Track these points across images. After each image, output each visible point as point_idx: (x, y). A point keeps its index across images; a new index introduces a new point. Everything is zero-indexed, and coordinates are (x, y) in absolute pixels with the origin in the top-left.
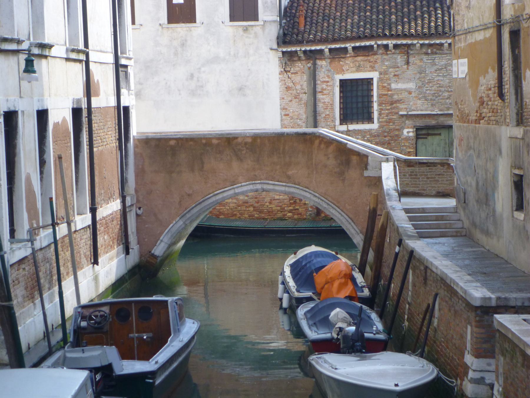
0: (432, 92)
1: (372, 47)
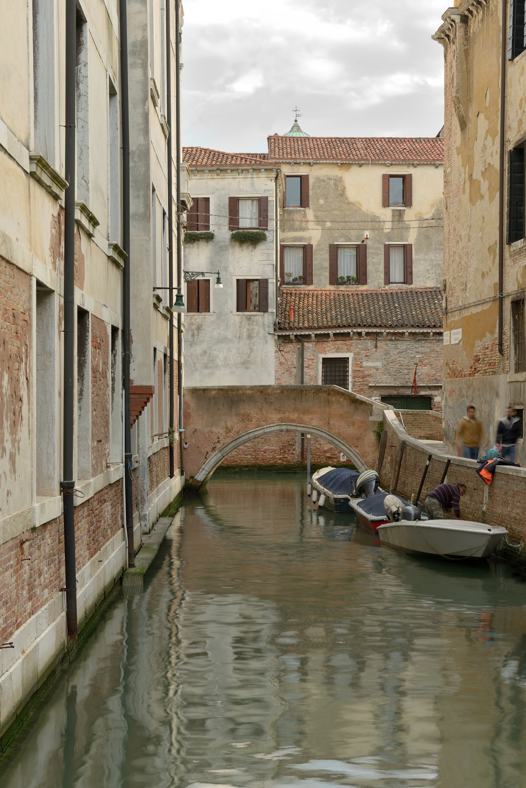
0: (395, 370)
1: (349, 333)
